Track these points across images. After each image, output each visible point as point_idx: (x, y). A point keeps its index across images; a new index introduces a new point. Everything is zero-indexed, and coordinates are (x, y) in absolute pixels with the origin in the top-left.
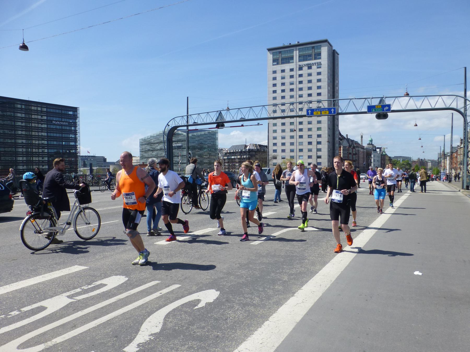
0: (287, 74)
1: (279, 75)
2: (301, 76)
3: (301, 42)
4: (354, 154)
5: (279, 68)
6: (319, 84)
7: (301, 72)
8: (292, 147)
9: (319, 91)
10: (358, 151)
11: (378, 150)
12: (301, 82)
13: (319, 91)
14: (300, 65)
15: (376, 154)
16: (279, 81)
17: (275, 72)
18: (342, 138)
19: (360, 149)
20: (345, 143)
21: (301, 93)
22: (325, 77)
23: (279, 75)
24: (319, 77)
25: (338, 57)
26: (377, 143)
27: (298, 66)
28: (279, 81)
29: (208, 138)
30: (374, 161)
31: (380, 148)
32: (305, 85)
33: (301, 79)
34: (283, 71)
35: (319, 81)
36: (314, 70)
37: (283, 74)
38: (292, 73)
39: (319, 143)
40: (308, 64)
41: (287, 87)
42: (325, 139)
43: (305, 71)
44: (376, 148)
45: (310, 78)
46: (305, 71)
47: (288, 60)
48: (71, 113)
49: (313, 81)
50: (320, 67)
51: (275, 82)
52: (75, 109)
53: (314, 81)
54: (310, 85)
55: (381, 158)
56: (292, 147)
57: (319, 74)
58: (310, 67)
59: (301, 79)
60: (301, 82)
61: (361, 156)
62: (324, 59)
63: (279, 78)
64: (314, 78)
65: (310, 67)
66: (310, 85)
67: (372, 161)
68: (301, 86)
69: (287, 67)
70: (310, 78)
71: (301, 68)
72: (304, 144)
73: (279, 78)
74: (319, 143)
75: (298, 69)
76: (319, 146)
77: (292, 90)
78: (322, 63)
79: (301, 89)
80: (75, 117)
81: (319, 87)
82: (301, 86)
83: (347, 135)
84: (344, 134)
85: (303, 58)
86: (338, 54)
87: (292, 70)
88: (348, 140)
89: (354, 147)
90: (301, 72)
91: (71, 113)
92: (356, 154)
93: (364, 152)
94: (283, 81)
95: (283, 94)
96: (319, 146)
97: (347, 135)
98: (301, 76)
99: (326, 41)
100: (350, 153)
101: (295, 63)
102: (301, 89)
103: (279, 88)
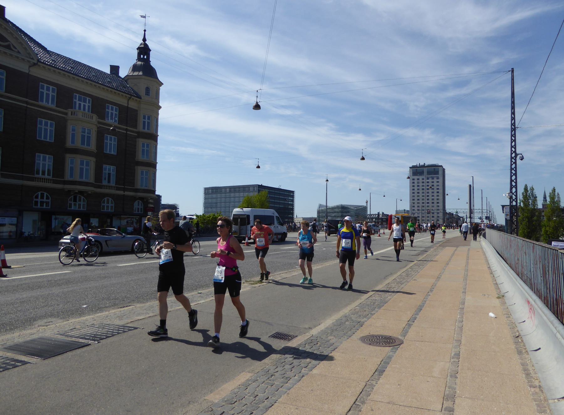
0: (421, 181)
1: (416, 181)
2: (428, 182)
3: (427, 164)
5: (416, 177)
7: (428, 181)
16: (416, 184)
23: (416, 181)
28: (416, 184)
34: (418, 179)
36: (435, 180)
41: (421, 188)
43: (430, 180)
46: (430, 180)
47: (421, 173)
52: (293, 192)
58: (433, 179)
64: (435, 184)
65: (433, 179)
69: (421, 178)
71: (428, 179)
77: (423, 189)
80: (293, 196)
81: (438, 189)
85: (429, 173)
87: (423, 179)
90: (428, 181)
99: (441, 166)
103: (416, 188)
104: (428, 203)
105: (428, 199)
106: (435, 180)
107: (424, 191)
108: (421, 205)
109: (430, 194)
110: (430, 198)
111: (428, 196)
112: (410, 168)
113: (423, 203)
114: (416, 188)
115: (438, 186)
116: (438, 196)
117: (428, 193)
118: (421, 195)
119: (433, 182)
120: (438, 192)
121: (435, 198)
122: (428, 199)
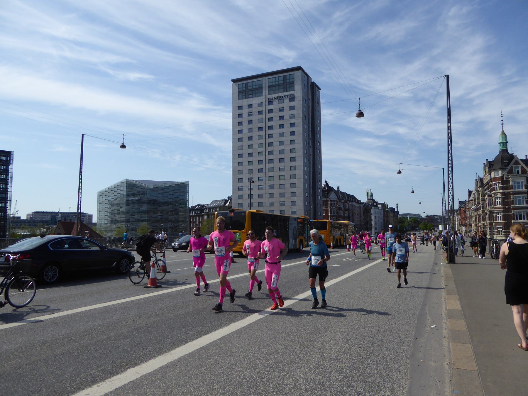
1: (245, 111)
2: (271, 111)
4: (346, 210)
5: (245, 102)
6: (292, 121)
7: (271, 107)
8: (261, 200)
9: (292, 129)
10: (353, 205)
11: (379, 206)
12: (270, 119)
13: (292, 129)
14: (269, 99)
15: (377, 210)
17: (240, 108)
18: (329, 189)
19: (354, 204)
20: (333, 196)
21: (271, 132)
22: (299, 112)
23: (245, 111)
24: (293, 112)
25: (319, 93)
26: (378, 198)
27: (267, 100)
28: (245, 119)
29: (176, 191)
30: (375, 218)
31: (383, 204)
32: (276, 123)
33: (271, 115)
34: (250, 106)
35: (292, 117)
36: (287, 103)
37: (250, 110)
38: (260, 109)
39: (293, 194)
40: (279, 98)
42: (300, 189)
43: (275, 106)
44: (377, 203)
45: (281, 114)
47: (257, 91)
48: (3, 158)
49: (285, 118)
50: (294, 101)
51: (240, 120)
52: (8, 154)
53: (286, 117)
54: (281, 122)
55: (384, 214)
56: (261, 200)
57: (292, 108)
59: (271, 115)
60: (270, 119)
61: (357, 211)
62: (298, 91)
63: (245, 115)
64: (286, 113)
66: (281, 122)
67: (373, 217)
68: (271, 123)
69: (254, 101)
70: (281, 114)
71: (270, 102)
72: (275, 196)
73: (245, 115)
74: (293, 194)
75: (267, 103)
76: (294, 199)
77: (260, 129)
78: (296, 95)
79: (271, 128)
81: (292, 125)
82: (271, 123)
83: (338, 187)
84: (333, 184)
85: (272, 88)
86: (320, 89)
87: (260, 105)
88: (338, 192)
89: (346, 202)
90: (271, 107)
91: (3, 158)
92: (348, 210)
93: (360, 207)
94: (250, 118)
95: (250, 134)
96: (294, 199)
97: (338, 187)
98: (271, 111)
99: (299, 68)
100: (340, 209)
101: (264, 97)
102: (271, 128)
104: (271, 161)
105: (271, 153)
106: (287, 103)
107: (262, 133)
108: (255, 167)
109: (276, 140)
110: (276, 148)
111: (271, 144)
112: (234, 81)
113: (260, 162)
114: (245, 127)
115: (292, 117)
116: (292, 142)
117: (271, 136)
118: (255, 142)
119: (281, 110)
120: (292, 133)
121: (287, 147)
122: (271, 153)
